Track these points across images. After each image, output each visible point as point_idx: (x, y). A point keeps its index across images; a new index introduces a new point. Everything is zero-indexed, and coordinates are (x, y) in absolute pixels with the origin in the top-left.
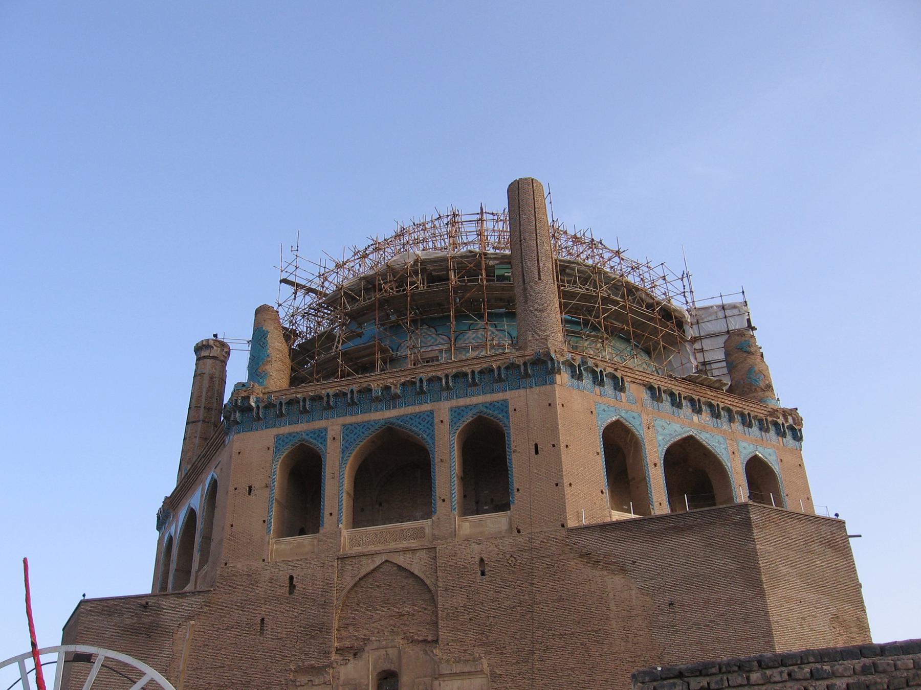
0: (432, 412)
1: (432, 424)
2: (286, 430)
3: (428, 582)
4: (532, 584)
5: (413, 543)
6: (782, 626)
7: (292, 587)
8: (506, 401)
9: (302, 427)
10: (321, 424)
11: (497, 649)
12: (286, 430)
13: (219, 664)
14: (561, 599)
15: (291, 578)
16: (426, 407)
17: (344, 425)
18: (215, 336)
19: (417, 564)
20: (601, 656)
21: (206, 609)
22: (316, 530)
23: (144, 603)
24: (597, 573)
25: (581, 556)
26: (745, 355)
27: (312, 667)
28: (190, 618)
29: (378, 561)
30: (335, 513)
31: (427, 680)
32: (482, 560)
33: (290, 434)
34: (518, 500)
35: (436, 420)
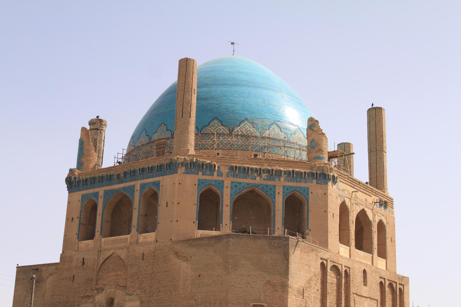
0: (134, 186)
1: (134, 192)
2: (85, 192)
3: (126, 262)
4: (158, 264)
5: (122, 245)
6: (235, 287)
7: (84, 263)
8: (159, 181)
9: (91, 191)
10: (96, 190)
11: (144, 291)
12: (85, 192)
13: (59, 294)
14: (166, 271)
15: (83, 259)
16: (132, 183)
17: (105, 191)
18: (98, 117)
19: (123, 254)
20: (175, 295)
21: (56, 271)
22: (93, 239)
23: (36, 268)
24: (179, 261)
25: (175, 253)
26: (311, 132)
27: (88, 296)
28: (51, 275)
29: (111, 252)
30: (99, 230)
31: (122, 302)
32: (143, 254)
33: (87, 194)
34: (159, 227)
35: (136, 190)
